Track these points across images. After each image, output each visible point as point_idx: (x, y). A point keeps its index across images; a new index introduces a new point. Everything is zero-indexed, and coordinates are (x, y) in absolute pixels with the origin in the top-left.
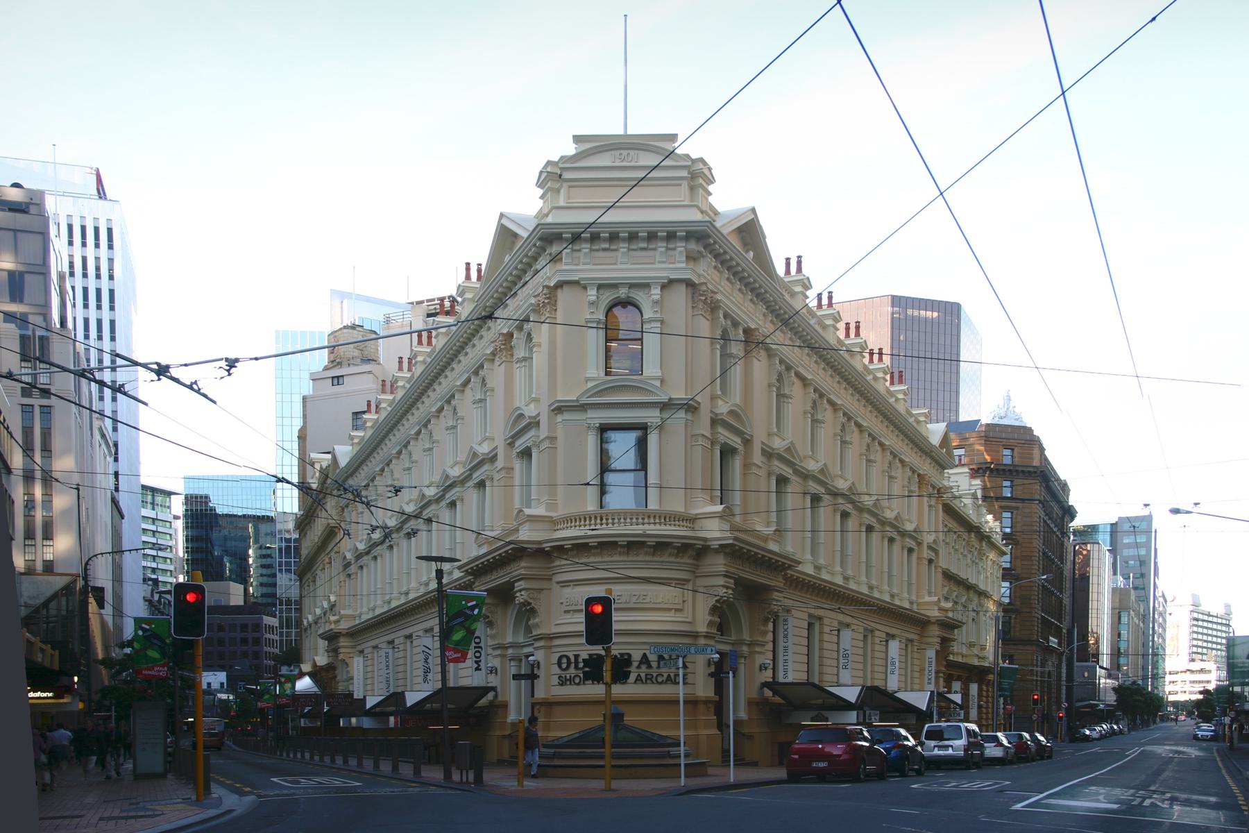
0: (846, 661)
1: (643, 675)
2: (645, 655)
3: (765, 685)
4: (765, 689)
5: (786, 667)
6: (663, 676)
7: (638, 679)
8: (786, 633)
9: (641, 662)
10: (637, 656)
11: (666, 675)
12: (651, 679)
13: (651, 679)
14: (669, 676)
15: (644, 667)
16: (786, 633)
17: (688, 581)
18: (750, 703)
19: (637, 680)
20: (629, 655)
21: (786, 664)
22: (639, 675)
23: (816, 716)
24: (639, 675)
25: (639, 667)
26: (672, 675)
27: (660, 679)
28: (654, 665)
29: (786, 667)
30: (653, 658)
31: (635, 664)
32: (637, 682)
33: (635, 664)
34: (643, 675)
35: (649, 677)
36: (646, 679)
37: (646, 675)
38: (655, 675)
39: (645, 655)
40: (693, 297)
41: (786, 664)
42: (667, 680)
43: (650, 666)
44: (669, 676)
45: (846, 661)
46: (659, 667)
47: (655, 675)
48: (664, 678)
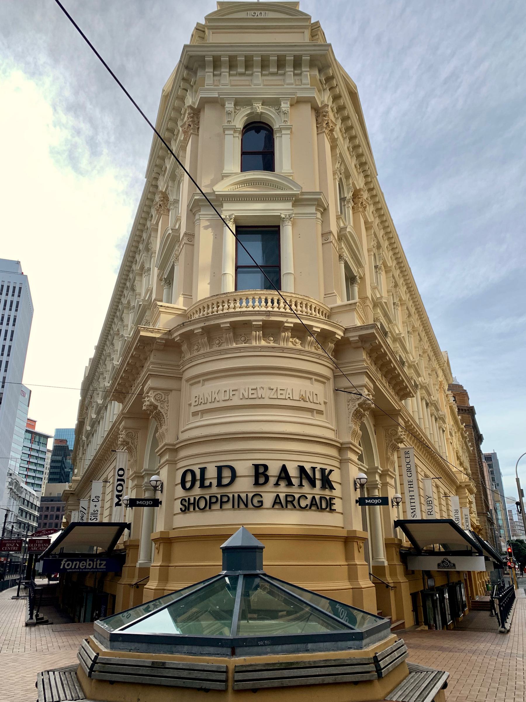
0: (431, 507)
1: (282, 496)
2: (284, 468)
3: (398, 523)
4: (398, 529)
5: (413, 504)
6: (307, 498)
7: (277, 502)
8: (408, 466)
9: (280, 478)
10: (274, 470)
11: (310, 497)
12: (292, 502)
13: (292, 502)
14: (314, 498)
15: (283, 484)
16: (408, 466)
17: (328, 379)
18: (388, 545)
19: (275, 503)
20: (266, 467)
21: (412, 501)
22: (278, 495)
23: (443, 562)
24: (278, 495)
25: (277, 484)
26: (317, 498)
27: (303, 503)
28: (295, 481)
29: (413, 504)
30: (293, 472)
31: (272, 480)
32: (276, 506)
33: (272, 480)
34: (282, 496)
35: (289, 499)
36: (287, 501)
37: (286, 496)
38: (297, 496)
39: (284, 468)
40: (317, 120)
41: (412, 501)
42: (312, 504)
43: (290, 484)
44: (314, 498)
45: (431, 507)
46: (301, 485)
47: (297, 496)
48: (308, 502)
